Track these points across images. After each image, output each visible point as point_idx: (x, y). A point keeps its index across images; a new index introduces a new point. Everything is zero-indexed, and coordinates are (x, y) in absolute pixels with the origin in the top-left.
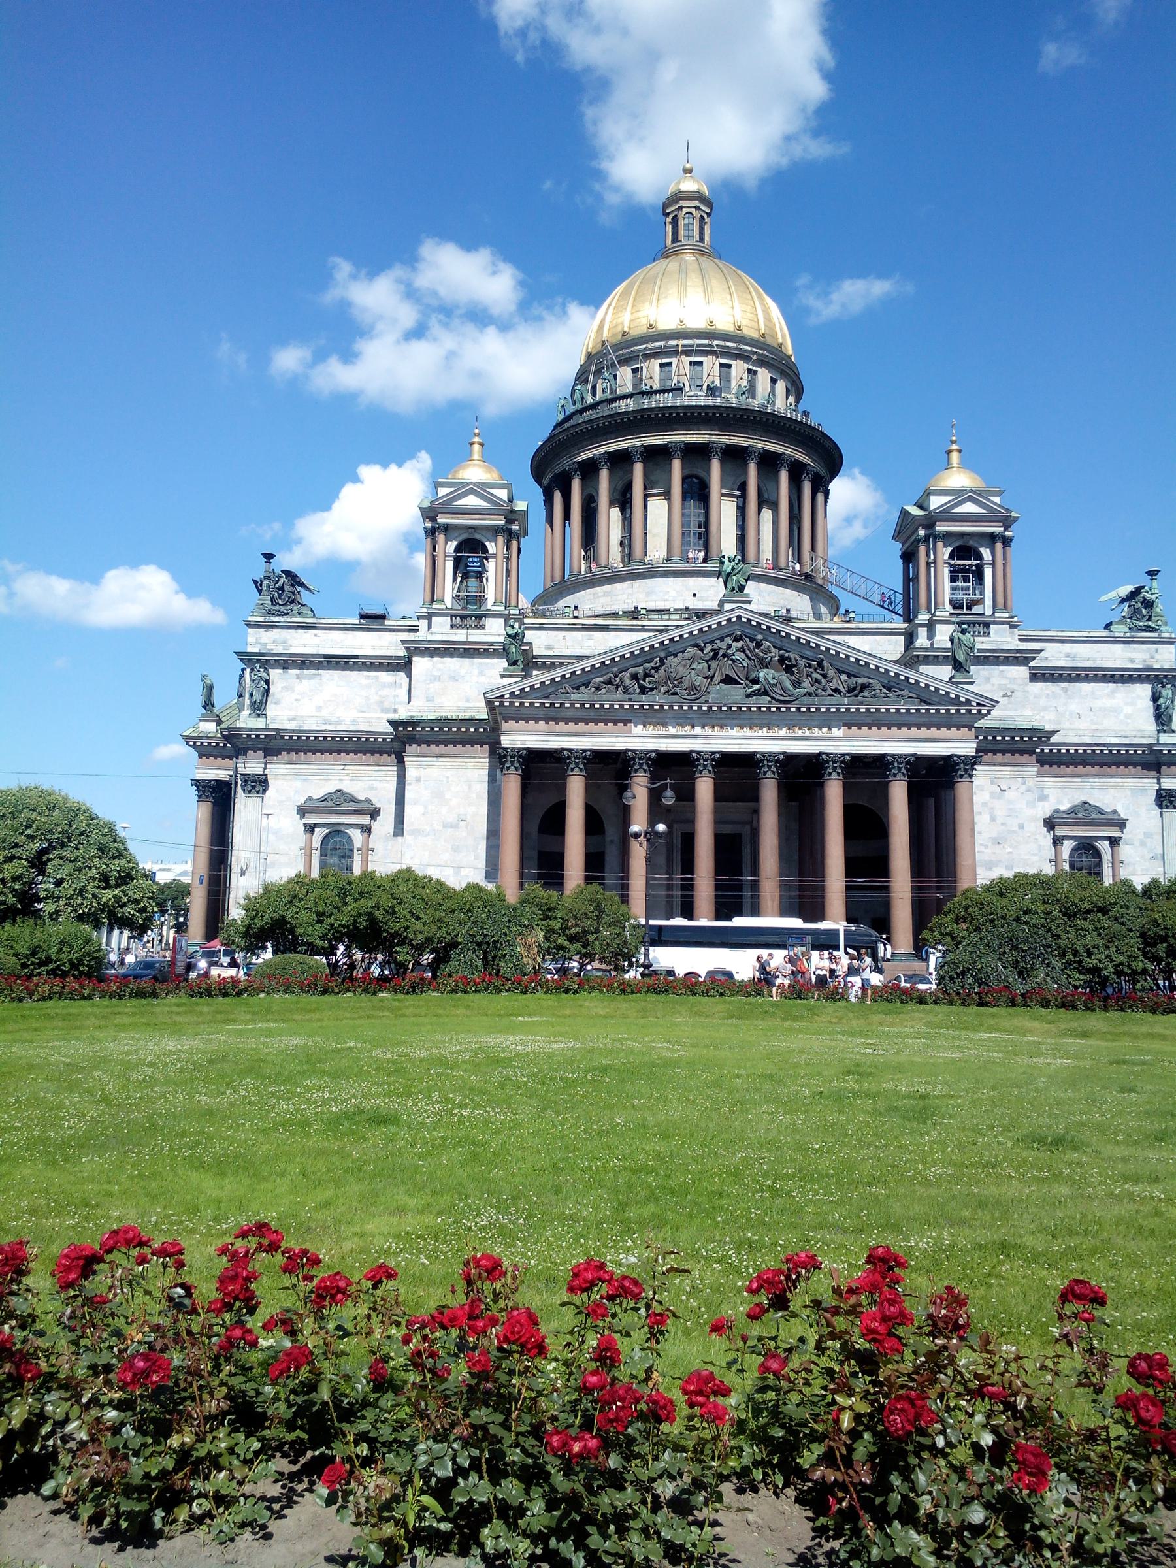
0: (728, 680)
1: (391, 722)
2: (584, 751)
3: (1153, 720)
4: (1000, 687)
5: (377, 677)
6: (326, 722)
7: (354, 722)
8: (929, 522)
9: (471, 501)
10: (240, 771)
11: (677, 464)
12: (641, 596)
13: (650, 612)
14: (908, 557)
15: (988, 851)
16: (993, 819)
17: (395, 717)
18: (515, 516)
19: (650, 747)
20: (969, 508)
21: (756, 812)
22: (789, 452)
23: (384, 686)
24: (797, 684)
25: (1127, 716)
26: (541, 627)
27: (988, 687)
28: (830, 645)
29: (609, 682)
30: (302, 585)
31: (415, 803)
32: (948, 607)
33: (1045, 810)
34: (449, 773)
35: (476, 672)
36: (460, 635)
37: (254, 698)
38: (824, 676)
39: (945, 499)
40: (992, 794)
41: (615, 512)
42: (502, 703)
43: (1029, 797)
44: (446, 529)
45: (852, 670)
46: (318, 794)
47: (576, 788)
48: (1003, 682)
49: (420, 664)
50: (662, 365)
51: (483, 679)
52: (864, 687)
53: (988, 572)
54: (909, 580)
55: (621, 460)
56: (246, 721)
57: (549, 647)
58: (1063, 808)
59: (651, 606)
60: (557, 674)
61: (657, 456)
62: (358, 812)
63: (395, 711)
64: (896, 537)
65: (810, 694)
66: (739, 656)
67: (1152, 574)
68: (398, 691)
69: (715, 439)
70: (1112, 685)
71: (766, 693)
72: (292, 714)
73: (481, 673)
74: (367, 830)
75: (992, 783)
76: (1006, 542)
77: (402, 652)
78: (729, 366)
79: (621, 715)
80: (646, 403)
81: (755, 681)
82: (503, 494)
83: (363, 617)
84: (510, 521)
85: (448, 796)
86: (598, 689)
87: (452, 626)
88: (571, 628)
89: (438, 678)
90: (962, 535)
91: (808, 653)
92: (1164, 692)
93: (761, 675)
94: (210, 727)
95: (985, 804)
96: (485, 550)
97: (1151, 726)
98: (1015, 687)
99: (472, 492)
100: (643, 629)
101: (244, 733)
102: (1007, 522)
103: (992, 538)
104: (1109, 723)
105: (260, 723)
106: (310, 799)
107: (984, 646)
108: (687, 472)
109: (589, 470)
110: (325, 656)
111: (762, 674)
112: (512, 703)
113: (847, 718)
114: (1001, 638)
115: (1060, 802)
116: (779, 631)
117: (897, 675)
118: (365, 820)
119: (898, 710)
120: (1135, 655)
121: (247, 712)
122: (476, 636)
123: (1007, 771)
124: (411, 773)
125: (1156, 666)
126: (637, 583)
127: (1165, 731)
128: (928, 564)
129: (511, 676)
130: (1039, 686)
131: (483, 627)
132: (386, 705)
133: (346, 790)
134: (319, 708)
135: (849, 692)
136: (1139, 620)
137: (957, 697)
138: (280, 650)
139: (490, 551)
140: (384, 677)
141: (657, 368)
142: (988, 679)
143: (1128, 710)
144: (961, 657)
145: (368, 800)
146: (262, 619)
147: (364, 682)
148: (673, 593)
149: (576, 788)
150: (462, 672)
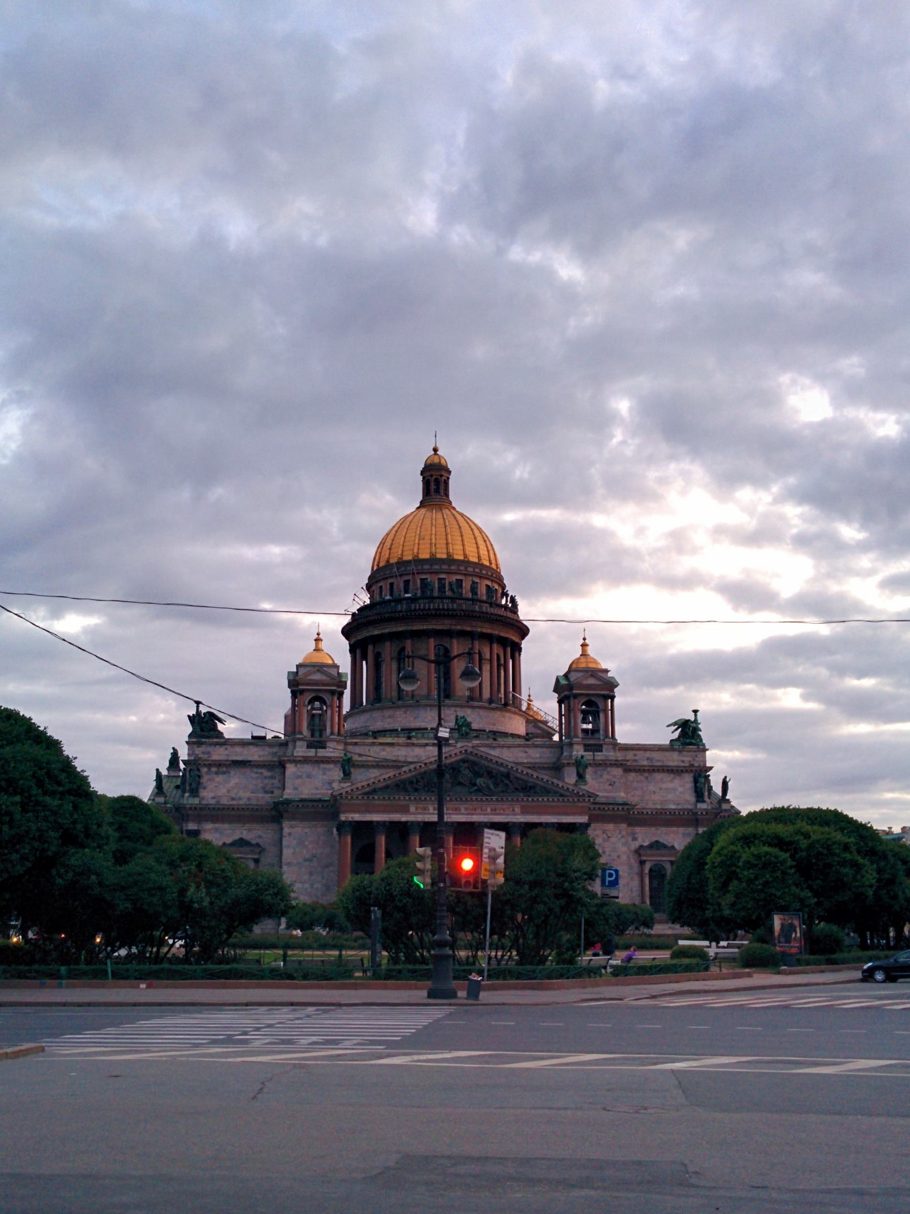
0: (460, 784)
2: (385, 822)
3: (694, 794)
4: (608, 780)
5: (261, 773)
6: (233, 799)
7: (249, 799)
8: (570, 687)
9: (317, 677)
10: (185, 828)
12: (412, 719)
14: (560, 702)
19: (420, 820)
20: (592, 681)
22: (496, 632)
23: (266, 778)
25: (681, 793)
26: (356, 744)
27: (601, 780)
28: (513, 765)
29: (398, 785)
31: (288, 847)
32: (580, 734)
33: (635, 845)
38: (511, 782)
39: (579, 675)
40: (604, 840)
43: (623, 840)
45: (525, 778)
46: (229, 841)
47: (381, 842)
48: (609, 777)
49: (291, 769)
50: (422, 580)
51: (325, 777)
52: (530, 787)
53: (602, 715)
54: (560, 715)
58: (645, 844)
62: (252, 852)
63: (272, 792)
64: (555, 690)
66: (466, 772)
67: (695, 712)
68: (274, 781)
69: (453, 627)
70: (672, 775)
71: (479, 790)
72: (213, 795)
73: (324, 774)
74: (257, 861)
78: (461, 580)
79: (406, 803)
81: (475, 785)
82: (333, 672)
85: (306, 843)
87: (308, 747)
88: (373, 744)
89: (300, 777)
90: (588, 695)
94: (161, 800)
95: (600, 845)
97: (691, 797)
99: (318, 671)
100: (413, 744)
101: (188, 806)
104: (670, 797)
105: (196, 801)
106: (224, 844)
107: (599, 758)
110: (233, 761)
111: (479, 781)
115: (644, 841)
118: (256, 857)
120: (684, 759)
123: (611, 826)
124: (286, 830)
125: (696, 765)
128: (569, 710)
130: (632, 776)
131: (325, 748)
132: (267, 788)
133: (245, 838)
134: (229, 791)
135: (523, 789)
138: (205, 757)
140: (266, 773)
141: (419, 582)
142: (601, 776)
143: (681, 789)
144: (581, 771)
146: (194, 740)
147: (254, 775)
148: (430, 718)
149: (381, 842)
150: (314, 773)
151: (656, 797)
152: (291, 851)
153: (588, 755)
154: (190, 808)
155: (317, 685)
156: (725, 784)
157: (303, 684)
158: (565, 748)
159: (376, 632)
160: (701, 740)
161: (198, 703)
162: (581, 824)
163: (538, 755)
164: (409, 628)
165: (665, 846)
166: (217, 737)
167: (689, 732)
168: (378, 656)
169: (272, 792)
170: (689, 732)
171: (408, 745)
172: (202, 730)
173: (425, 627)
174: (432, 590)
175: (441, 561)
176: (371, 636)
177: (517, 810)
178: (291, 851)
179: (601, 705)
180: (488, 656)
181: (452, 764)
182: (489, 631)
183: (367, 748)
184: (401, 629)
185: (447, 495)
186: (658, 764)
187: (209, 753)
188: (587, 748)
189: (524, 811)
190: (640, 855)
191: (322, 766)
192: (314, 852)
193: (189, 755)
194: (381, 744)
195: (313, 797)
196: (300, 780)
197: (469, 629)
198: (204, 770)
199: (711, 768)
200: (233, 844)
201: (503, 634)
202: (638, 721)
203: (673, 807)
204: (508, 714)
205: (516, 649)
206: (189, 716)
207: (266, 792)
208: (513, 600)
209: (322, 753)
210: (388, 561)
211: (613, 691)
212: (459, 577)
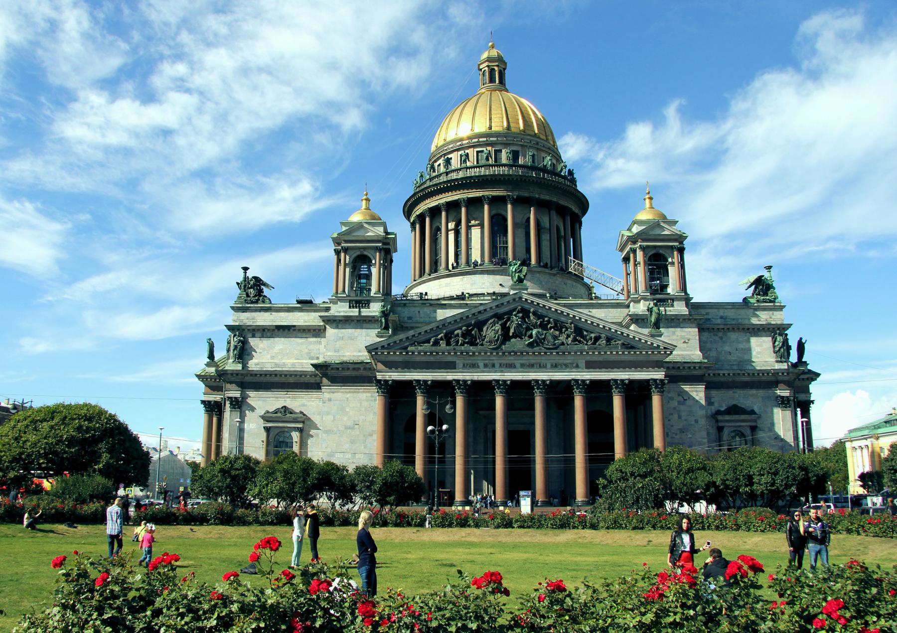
0: (515, 336)
1: (312, 365)
4: (682, 337)
6: (277, 365)
7: (293, 364)
11: (486, 207)
12: (468, 286)
13: (471, 295)
14: (626, 260)
15: (678, 437)
16: (680, 417)
17: (315, 362)
18: (388, 241)
19: (468, 378)
21: (533, 416)
22: (555, 200)
24: (555, 338)
27: (675, 337)
28: (575, 313)
29: (442, 339)
30: (265, 284)
34: (348, 395)
35: (364, 334)
36: (355, 312)
40: (679, 403)
41: (451, 236)
42: (376, 353)
44: (346, 250)
50: (478, 152)
51: (368, 338)
52: (597, 339)
55: (453, 206)
57: (410, 318)
58: (722, 409)
59: (471, 292)
60: (411, 333)
61: (474, 204)
62: (295, 421)
63: (318, 358)
67: (769, 268)
73: (367, 335)
75: (679, 395)
76: (681, 251)
77: (322, 324)
78: (518, 152)
79: (450, 359)
80: (469, 173)
81: (531, 336)
83: (299, 302)
84: (384, 244)
86: (436, 343)
87: (350, 307)
89: (342, 338)
90: (655, 247)
91: (563, 319)
92: (778, 339)
93: (534, 333)
95: (675, 408)
98: (690, 337)
102: (681, 238)
103: (672, 247)
106: (268, 412)
108: (494, 212)
109: (435, 212)
111: (534, 332)
112: (382, 353)
113: (588, 358)
114: (679, 308)
116: (544, 306)
117: (616, 331)
118: (300, 425)
119: (617, 353)
121: (231, 361)
122: (365, 312)
125: (773, 323)
127: (781, 362)
128: (635, 265)
129: (382, 337)
130: (706, 334)
132: (312, 355)
134: (273, 358)
136: (763, 295)
137: (652, 344)
142: (674, 333)
145: (301, 413)
148: (487, 284)
150: (356, 334)
151: (732, 358)
152: (330, 418)
157: (346, 242)
161: (246, 269)
162: (655, 380)
163: (603, 315)
164: (465, 196)
165: (743, 411)
166: (263, 302)
169: (318, 358)
171: (460, 306)
172: (248, 296)
174: (487, 159)
175: (497, 135)
176: (430, 209)
177: (582, 363)
178: (330, 418)
179: (670, 260)
180: (547, 225)
181: (505, 314)
182: (547, 198)
183: (417, 309)
184: (455, 198)
185: (502, 81)
189: (591, 365)
190: (717, 421)
191: (365, 325)
192: (356, 419)
195: (356, 360)
196: (341, 342)
197: (526, 194)
199: (789, 325)
200: (276, 412)
201: (562, 202)
204: (569, 282)
205: (576, 222)
206: (238, 284)
207: (312, 358)
208: (571, 173)
209: (365, 312)
210: (445, 140)
211: (681, 243)
212: (515, 148)
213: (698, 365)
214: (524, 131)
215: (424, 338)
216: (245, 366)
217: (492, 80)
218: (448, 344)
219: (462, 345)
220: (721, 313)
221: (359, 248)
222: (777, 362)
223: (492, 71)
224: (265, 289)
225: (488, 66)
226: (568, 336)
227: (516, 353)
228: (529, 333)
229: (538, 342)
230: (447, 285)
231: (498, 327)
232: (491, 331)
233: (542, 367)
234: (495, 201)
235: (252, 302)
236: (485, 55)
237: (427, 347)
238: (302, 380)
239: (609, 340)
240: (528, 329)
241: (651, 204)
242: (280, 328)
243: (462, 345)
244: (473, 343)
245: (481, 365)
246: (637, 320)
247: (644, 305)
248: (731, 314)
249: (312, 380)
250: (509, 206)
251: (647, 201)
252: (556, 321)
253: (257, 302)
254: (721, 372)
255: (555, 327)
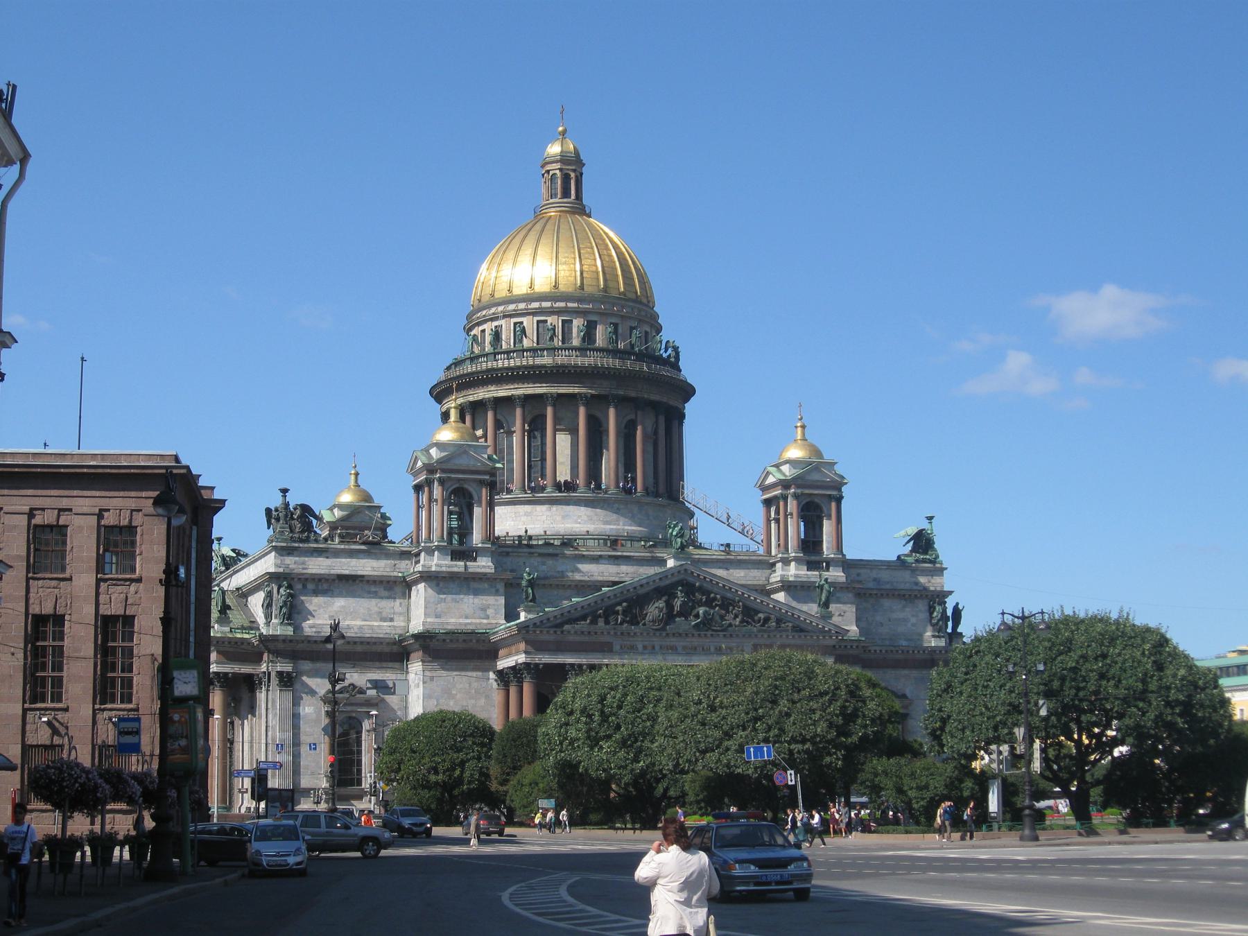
0: (680, 614)
7: (361, 627)
9: (463, 462)
11: (582, 411)
12: (559, 518)
14: (767, 503)
20: (815, 477)
22: (665, 400)
24: (722, 618)
25: (913, 625)
37: (284, 610)
52: (767, 620)
54: (768, 521)
56: (277, 628)
65: (730, 625)
67: (930, 518)
70: (903, 602)
76: (839, 500)
81: (697, 616)
86: (594, 622)
96: (471, 497)
102: (838, 485)
104: (901, 629)
105: (289, 631)
111: (701, 610)
114: (836, 574)
126: (554, 508)
132: (384, 615)
139: (476, 497)
143: (913, 620)
153: (813, 575)
154: (284, 641)
155: (463, 472)
156: (957, 613)
157: (443, 471)
158: (779, 565)
159: (502, 393)
160: (937, 557)
161: (284, 491)
166: (316, 541)
167: (922, 542)
168: (498, 425)
169: (392, 620)
170: (922, 542)
173: (576, 391)
179: (825, 509)
186: (888, 586)
187: (303, 563)
188: (812, 566)
191: (474, 585)
193: (277, 566)
194: (540, 555)
197: (633, 394)
198: (299, 586)
199: (951, 593)
202: (870, 531)
203: (904, 643)
211: (840, 490)
213: (855, 645)
214: (623, 293)
215: (578, 615)
216: (298, 628)
217: (566, 194)
218: (607, 622)
219: (622, 623)
220: (874, 574)
221: (459, 480)
222: (934, 636)
223: (566, 178)
224: (314, 522)
225: (561, 170)
226: (736, 616)
227: (680, 635)
228: (694, 612)
229: (706, 624)
230: (527, 514)
231: (661, 604)
232: (654, 610)
233: (706, 651)
234: (590, 401)
235: (301, 541)
236: (554, 149)
237: (584, 625)
238: (374, 648)
239: (779, 621)
240: (693, 608)
241: (803, 434)
242: (342, 578)
243: (622, 623)
244: (634, 621)
245: (640, 647)
246: (787, 586)
247: (797, 569)
248: (885, 575)
249: (387, 649)
250: (612, 412)
251: (799, 430)
252: (723, 598)
253: (307, 540)
254: (873, 649)
255: (722, 607)
